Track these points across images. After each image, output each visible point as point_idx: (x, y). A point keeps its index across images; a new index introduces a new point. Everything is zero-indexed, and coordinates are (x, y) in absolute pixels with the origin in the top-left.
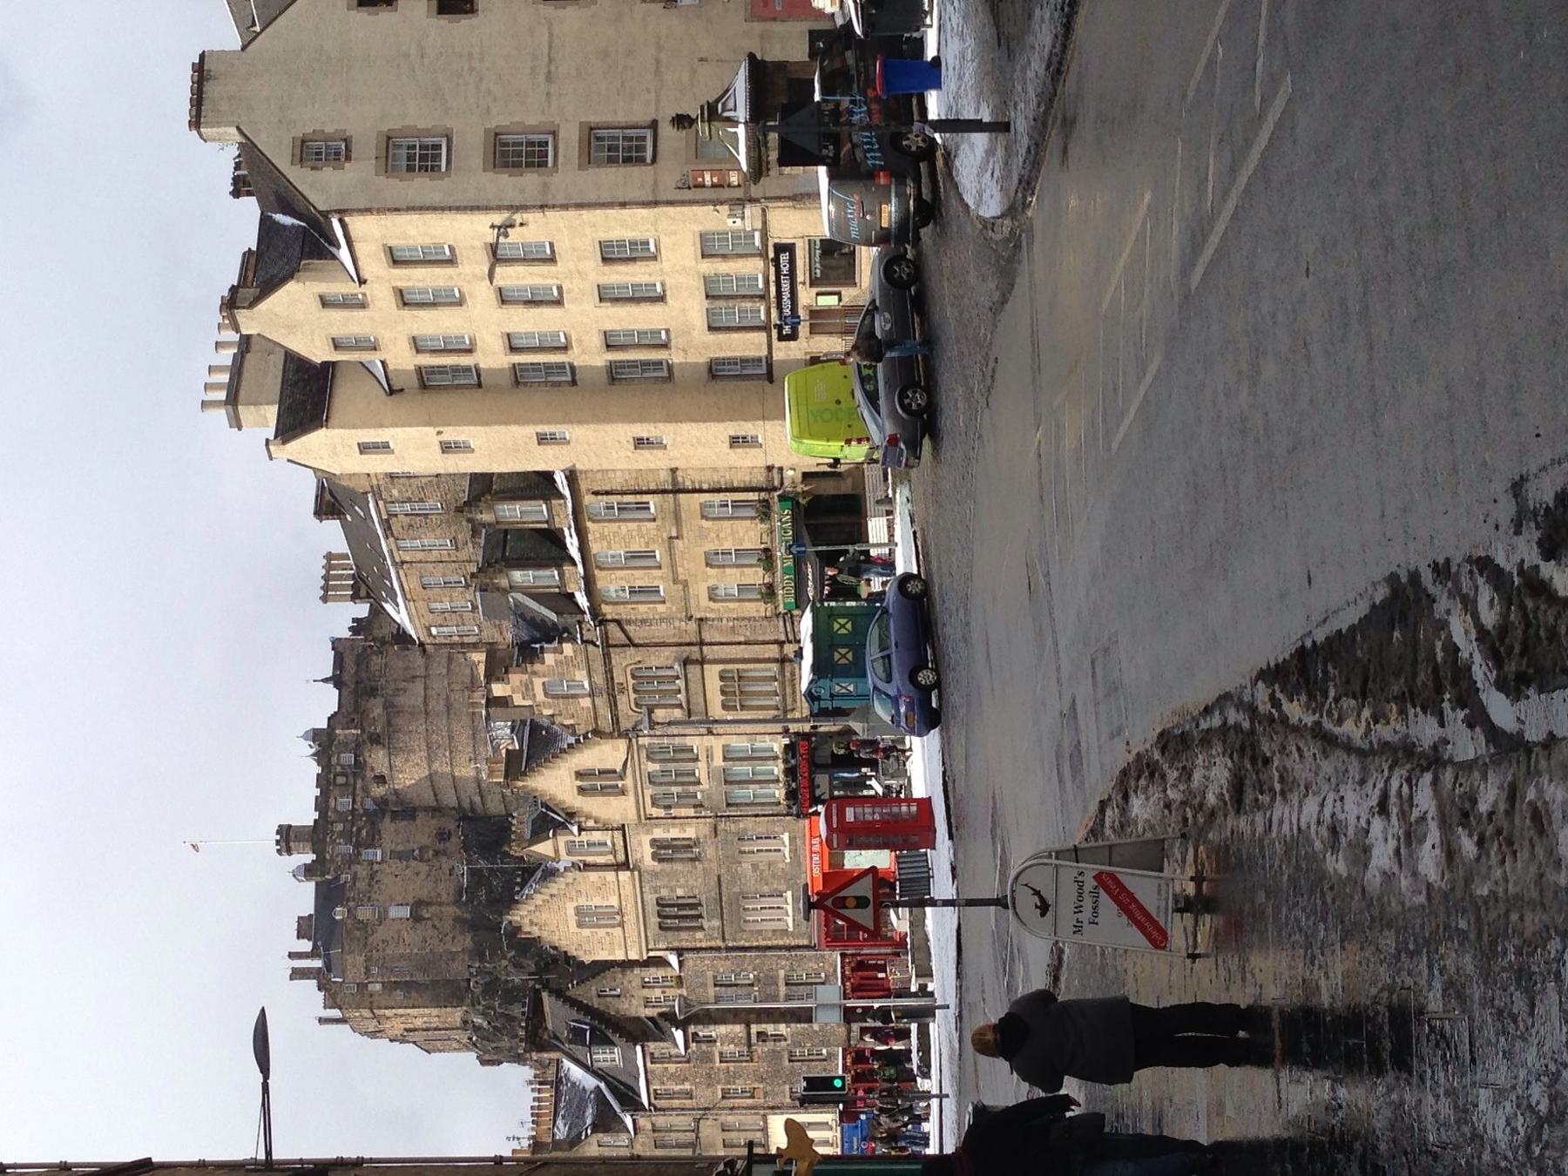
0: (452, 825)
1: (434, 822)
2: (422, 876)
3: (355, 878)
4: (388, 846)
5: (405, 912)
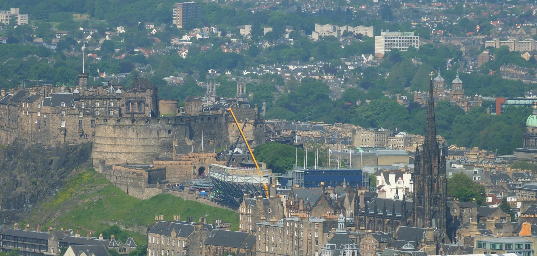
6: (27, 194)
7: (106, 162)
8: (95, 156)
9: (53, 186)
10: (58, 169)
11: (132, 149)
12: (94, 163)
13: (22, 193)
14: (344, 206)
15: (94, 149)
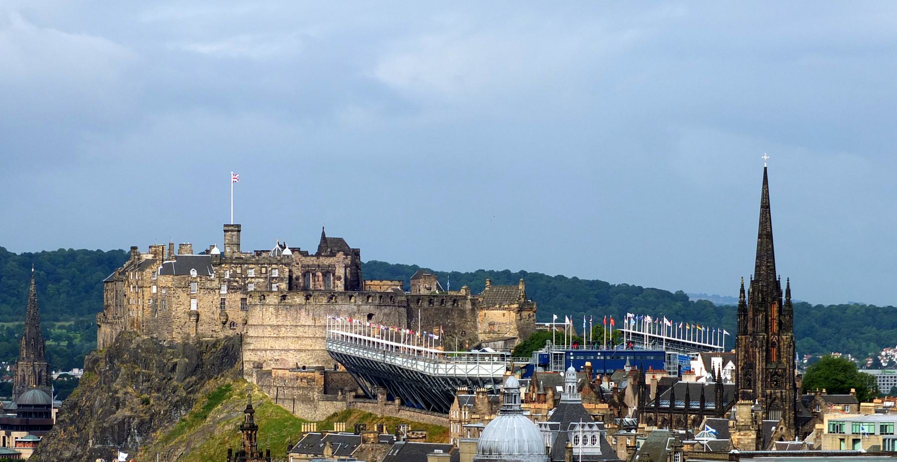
0: (238, 331)
1: (240, 320)
2: (212, 316)
3: (211, 280)
4: (227, 297)
5: (194, 308)
6: (134, 419)
7: (264, 365)
8: (248, 356)
9: (176, 406)
10: (185, 379)
11: (307, 344)
12: (245, 369)
13: (125, 417)
14: (625, 401)
15: (245, 347)
